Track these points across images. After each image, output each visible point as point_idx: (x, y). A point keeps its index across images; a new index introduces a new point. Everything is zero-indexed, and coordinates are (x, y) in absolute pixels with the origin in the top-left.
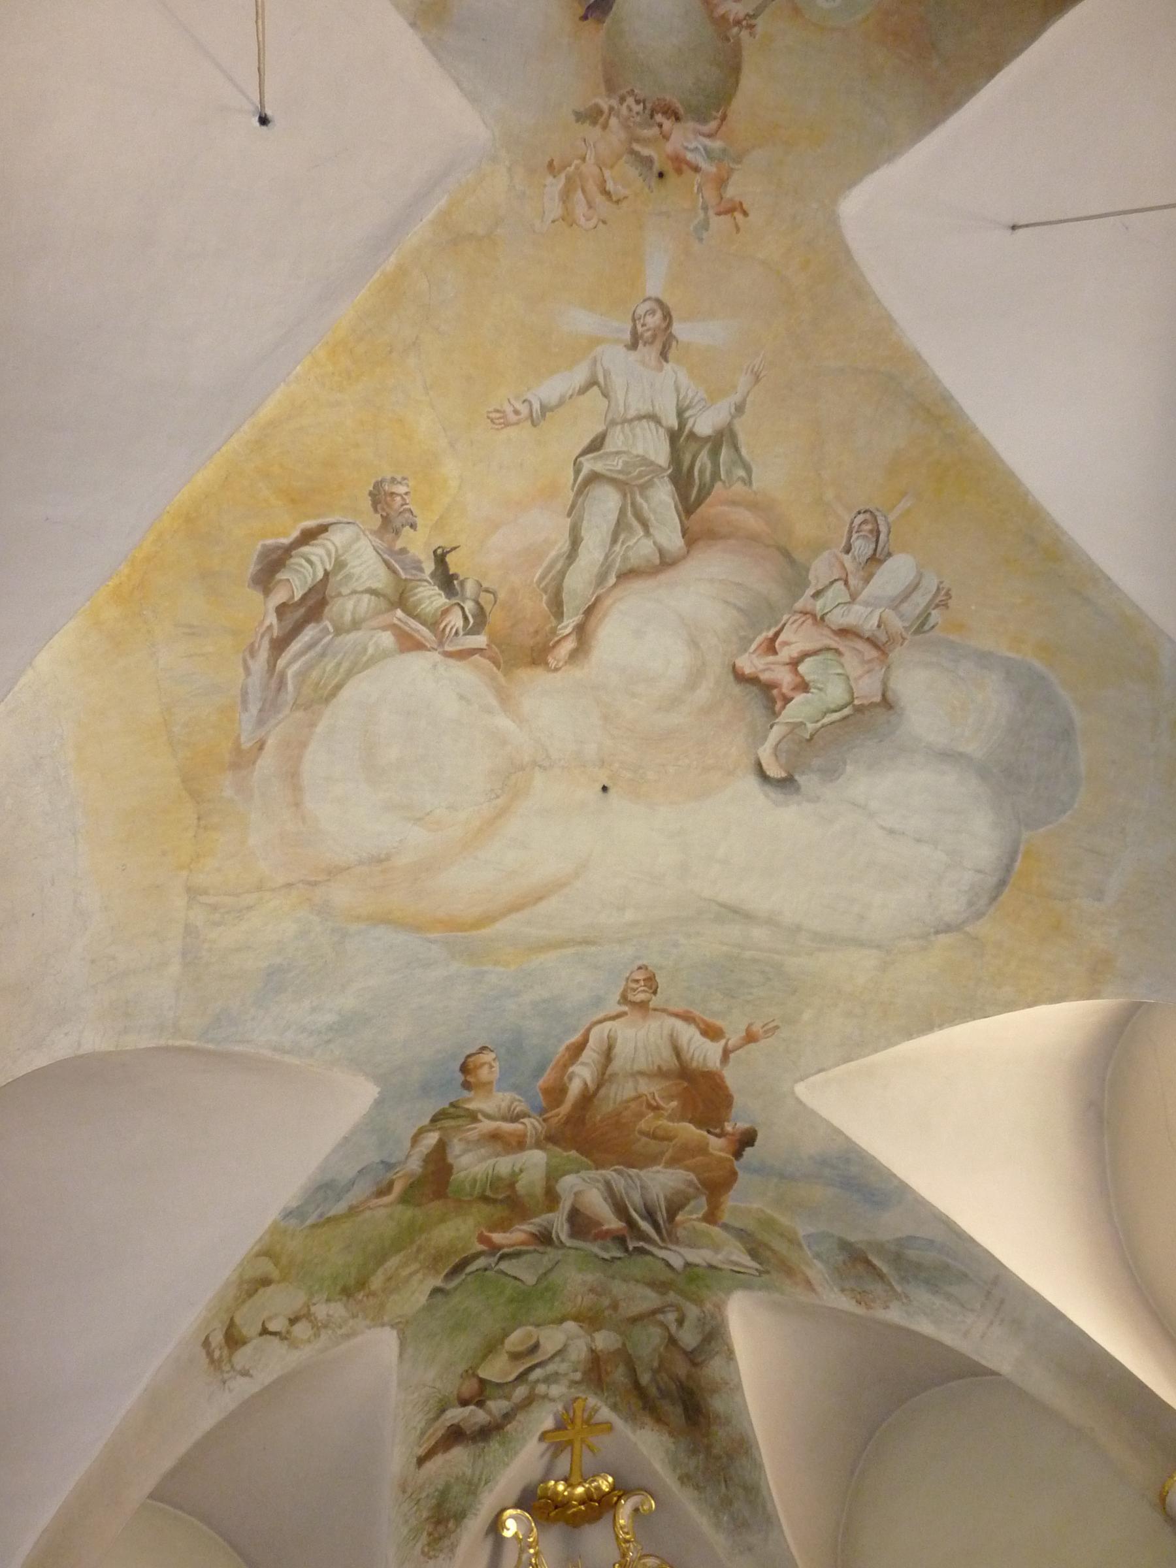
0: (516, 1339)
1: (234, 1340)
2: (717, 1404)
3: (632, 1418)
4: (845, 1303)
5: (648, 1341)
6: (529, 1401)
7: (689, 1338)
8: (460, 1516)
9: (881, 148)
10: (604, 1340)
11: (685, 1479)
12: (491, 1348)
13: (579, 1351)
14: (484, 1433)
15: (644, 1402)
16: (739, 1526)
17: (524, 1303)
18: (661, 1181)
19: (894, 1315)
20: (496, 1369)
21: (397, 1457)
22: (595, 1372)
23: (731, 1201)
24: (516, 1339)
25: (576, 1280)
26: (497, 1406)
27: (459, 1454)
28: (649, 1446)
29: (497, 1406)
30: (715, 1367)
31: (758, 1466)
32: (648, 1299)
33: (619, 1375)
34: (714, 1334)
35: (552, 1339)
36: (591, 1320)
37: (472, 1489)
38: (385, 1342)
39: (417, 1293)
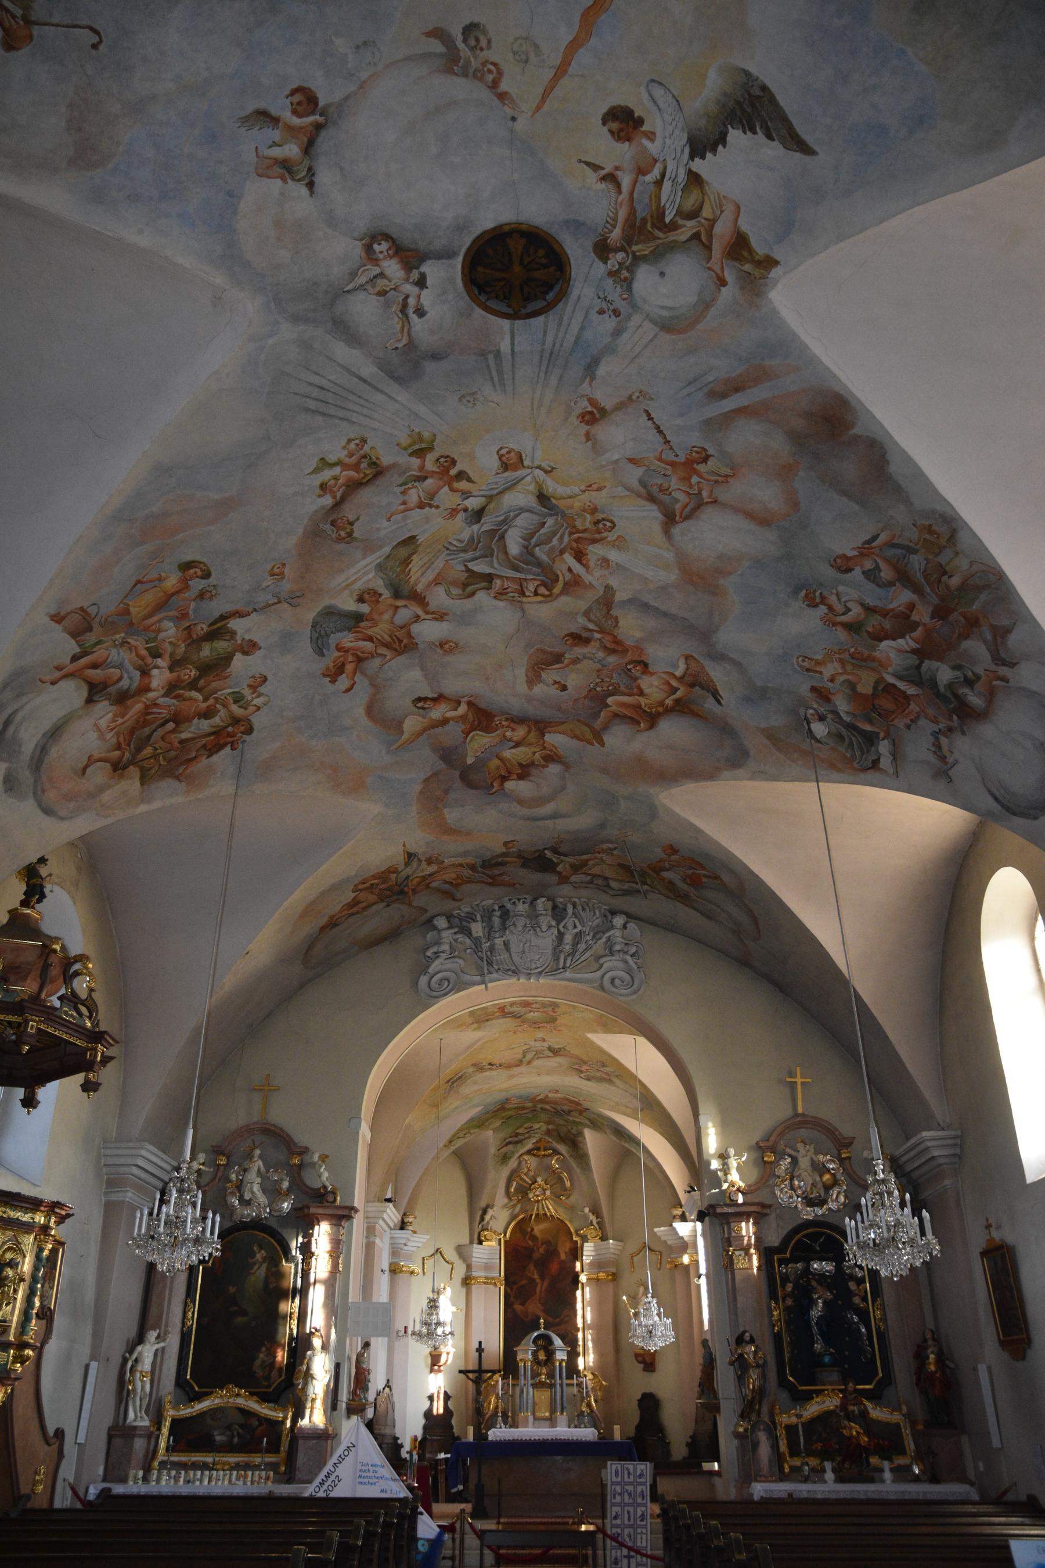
0: (526, 1125)
1: (450, 1142)
2: (581, 1145)
3: (558, 1142)
4: (615, 1139)
5: (563, 1130)
6: (529, 1137)
7: (574, 1131)
8: (510, 1158)
9: (595, 1031)
10: (550, 1127)
11: (571, 1156)
12: (518, 1128)
13: (544, 1128)
14: (517, 1142)
15: (562, 1139)
16: (583, 1168)
17: (528, 1120)
18: (566, 1108)
19: (626, 1145)
20: (520, 1131)
21: (493, 1150)
22: (548, 1132)
23: (584, 1114)
24: (526, 1125)
25: (544, 1116)
26: (520, 1137)
27: (510, 1147)
28: (562, 1148)
29: (520, 1137)
30: (580, 1139)
31: (589, 1159)
32: (562, 1122)
33: (555, 1133)
34: (581, 1134)
35: (536, 1126)
36: (548, 1123)
37: (513, 1153)
38: (491, 1132)
39: (498, 1123)
